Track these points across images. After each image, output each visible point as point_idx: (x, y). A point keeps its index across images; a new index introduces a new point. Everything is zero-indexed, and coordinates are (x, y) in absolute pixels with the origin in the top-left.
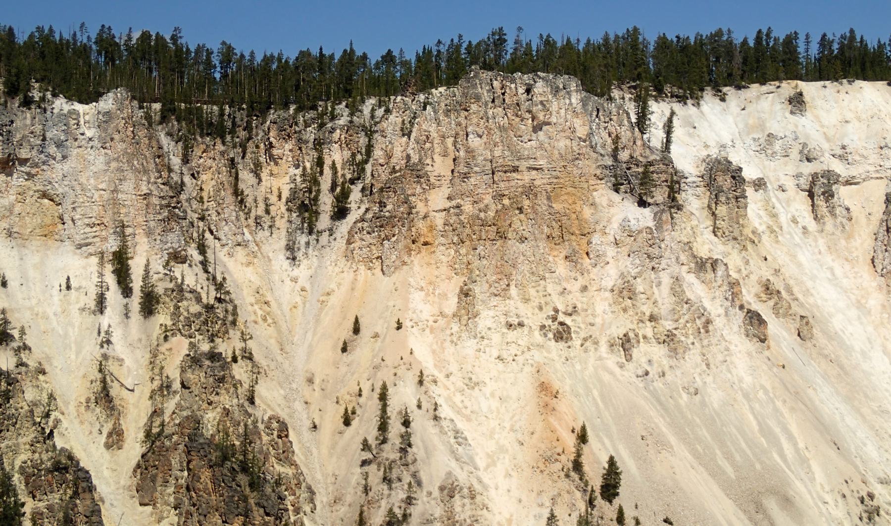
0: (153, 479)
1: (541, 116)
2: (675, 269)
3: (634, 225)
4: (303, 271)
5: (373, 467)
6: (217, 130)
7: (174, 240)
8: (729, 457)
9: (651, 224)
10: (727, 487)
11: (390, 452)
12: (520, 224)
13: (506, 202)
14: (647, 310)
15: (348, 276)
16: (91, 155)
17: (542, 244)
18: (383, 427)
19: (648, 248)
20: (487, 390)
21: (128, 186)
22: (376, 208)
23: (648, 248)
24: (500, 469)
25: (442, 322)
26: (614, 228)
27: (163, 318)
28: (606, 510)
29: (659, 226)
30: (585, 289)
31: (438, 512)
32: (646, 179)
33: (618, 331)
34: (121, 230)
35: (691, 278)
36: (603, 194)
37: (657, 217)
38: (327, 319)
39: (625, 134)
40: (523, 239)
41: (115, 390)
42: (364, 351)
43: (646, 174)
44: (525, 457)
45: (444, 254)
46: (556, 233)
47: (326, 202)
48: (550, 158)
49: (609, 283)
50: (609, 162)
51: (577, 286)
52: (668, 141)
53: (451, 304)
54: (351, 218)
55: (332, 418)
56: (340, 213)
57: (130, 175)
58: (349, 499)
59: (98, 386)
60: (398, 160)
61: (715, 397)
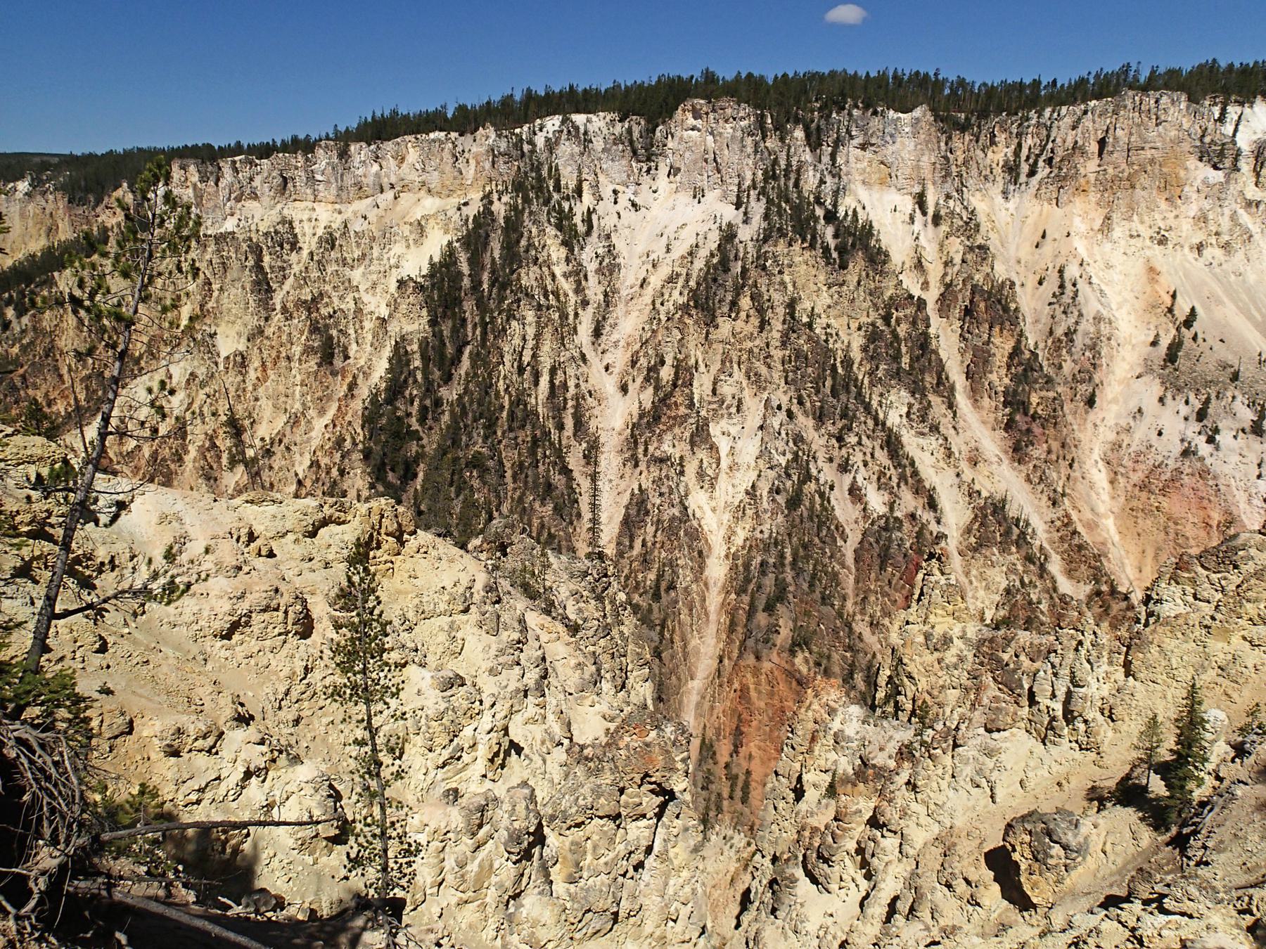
0: (949, 306)
1: (1163, 118)
2: (1234, 206)
3: (1211, 181)
4: (1011, 205)
5: (1056, 306)
6: (963, 128)
7: (949, 187)
8: (1259, 310)
9: (1223, 180)
10: (1257, 325)
11: (1066, 299)
12: (1143, 180)
13: (1136, 167)
14: (1214, 229)
15: (1037, 208)
16: (907, 141)
17: (1154, 192)
18: (1062, 286)
19: (1218, 194)
20: (1119, 268)
21: (925, 158)
22: (1056, 171)
23: (1218, 194)
24: (1124, 311)
25: (1091, 233)
26: (1198, 183)
27: (944, 228)
28: (1187, 334)
29: (1227, 182)
30: (1177, 216)
31: (1092, 329)
32: (1221, 154)
33: (1196, 241)
34: (922, 182)
35: (1241, 212)
36: (1192, 162)
37: (1227, 176)
38: (1027, 230)
39: (1211, 126)
40: (1144, 189)
41: (924, 263)
42: (1048, 248)
43: (1222, 150)
44: (1140, 305)
45: (1093, 197)
46: (1162, 185)
47: (1025, 168)
48: (1164, 142)
49: (1192, 214)
50: (1198, 144)
51: (1173, 215)
52: (1236, 130)
53: (1097, 224)
54: (1038, 177)
55: (1032, 281)
56: (1032, 173)
57: (927, 152)
58: (1043, 321)
59: (916, 260)
60: (1069, 144)
61: (1252, 278)
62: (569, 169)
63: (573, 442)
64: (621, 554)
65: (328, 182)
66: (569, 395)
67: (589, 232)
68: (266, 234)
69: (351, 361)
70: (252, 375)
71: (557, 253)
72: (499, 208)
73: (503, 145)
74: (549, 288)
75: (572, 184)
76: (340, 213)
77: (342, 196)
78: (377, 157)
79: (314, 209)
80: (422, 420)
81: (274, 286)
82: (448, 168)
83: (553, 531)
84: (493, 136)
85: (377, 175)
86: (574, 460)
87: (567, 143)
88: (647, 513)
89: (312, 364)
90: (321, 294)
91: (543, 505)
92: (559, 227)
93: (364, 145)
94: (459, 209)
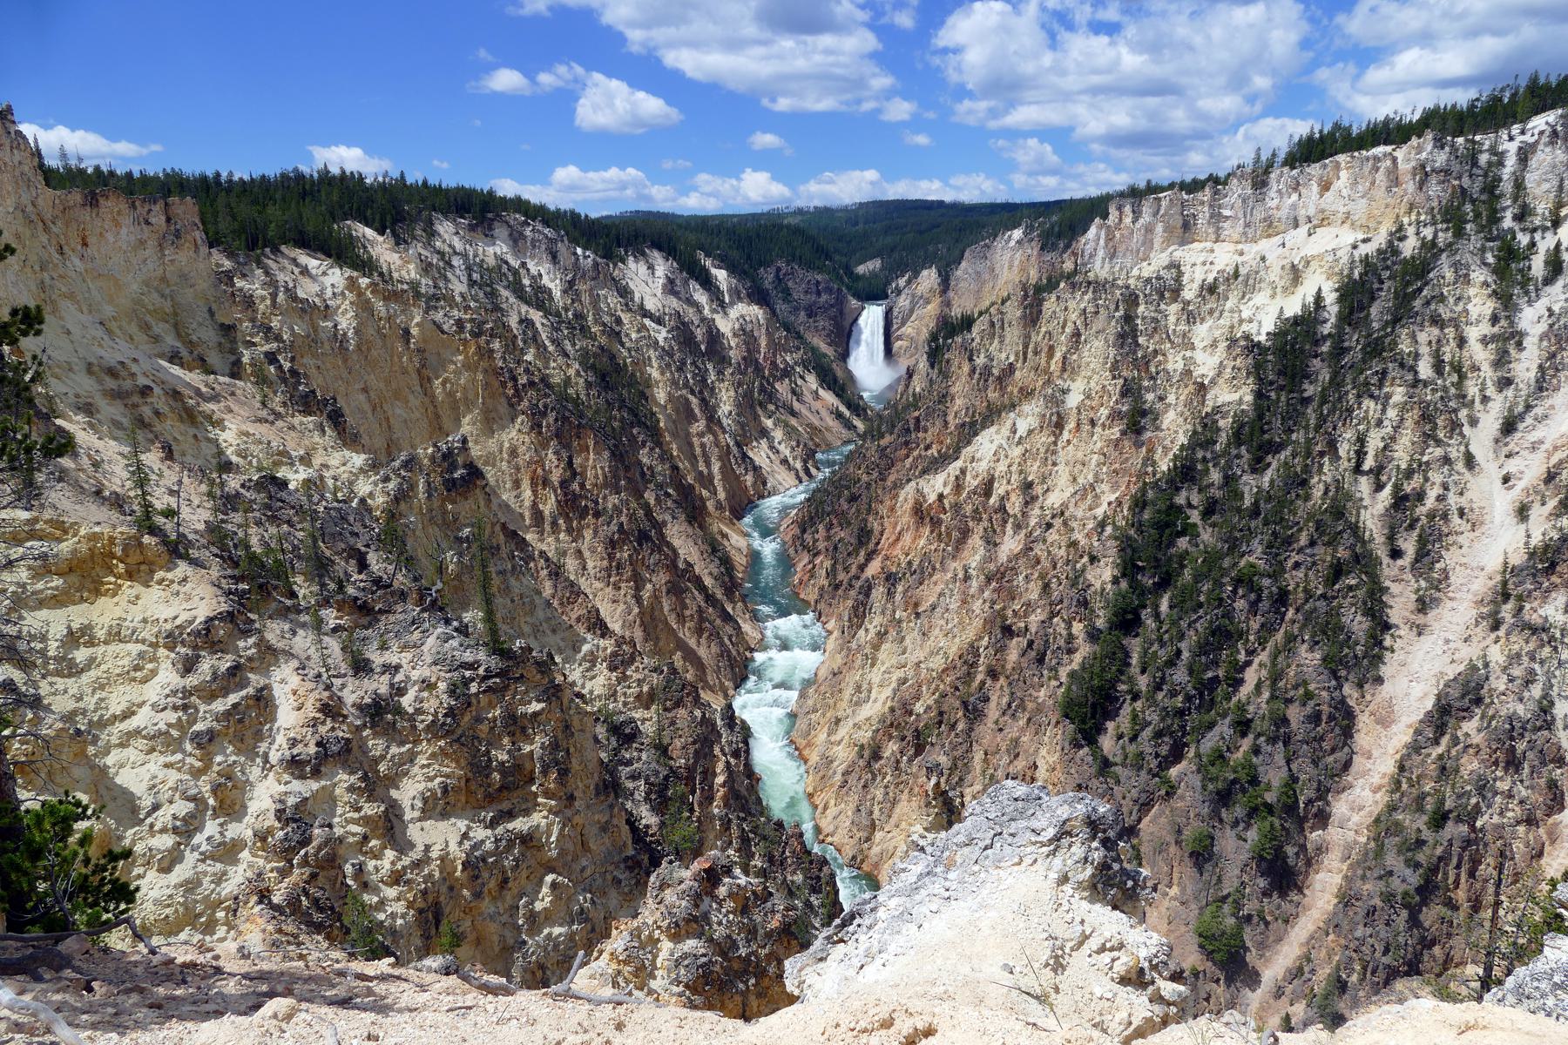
62: (1546, 186)
63: (1408, 576)
64: (1415, 748)
65: (1236, 218)
66: (1421, 510)
67: (1549, 281)
68: (1148, 280)
69: (1161, 434)
70: (1066, 435)
71: (1480, 305)
72: (1409, 247)
73: (1441, 158)
74: (1447, 358)
75: (1542, 207)
76: (1241, 254)
77: (1246, 238)
78: (1298, 184)
79: (1212, 251)
80: (1208, 512)
81: (1141, 340)
82: (1380, 193)
83: (1312, 687)
84: (1429, 147)
85: (1294, 207)
86: (1400, 602)
87: (1548, 150)
88: (1478, 701)
89: (1115, 432)
90: (1155, 351)
91: (1311, 650)
92: (1500, 271)
93: (1286, 169)
94: (1355, 247)
